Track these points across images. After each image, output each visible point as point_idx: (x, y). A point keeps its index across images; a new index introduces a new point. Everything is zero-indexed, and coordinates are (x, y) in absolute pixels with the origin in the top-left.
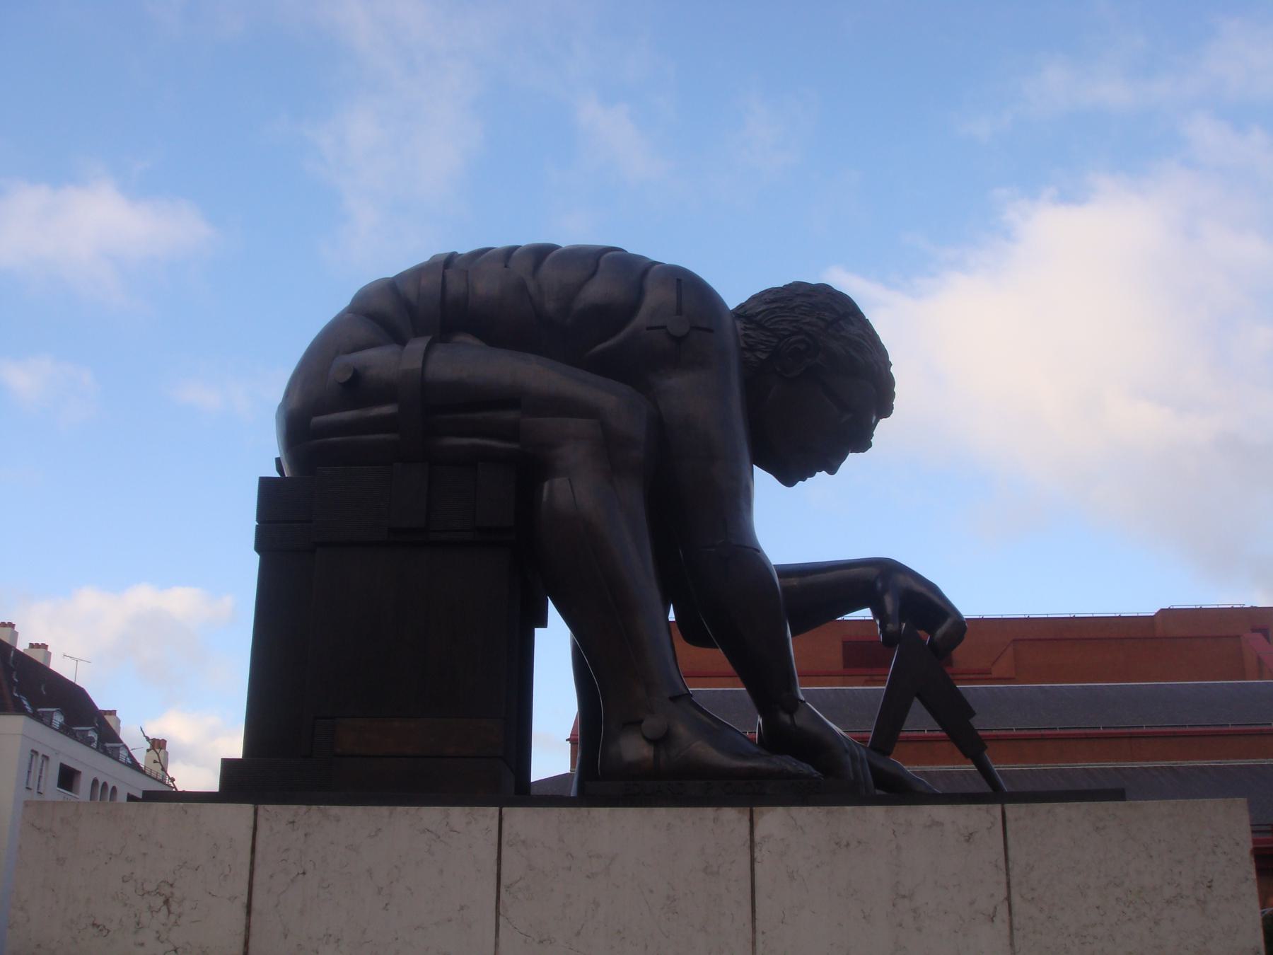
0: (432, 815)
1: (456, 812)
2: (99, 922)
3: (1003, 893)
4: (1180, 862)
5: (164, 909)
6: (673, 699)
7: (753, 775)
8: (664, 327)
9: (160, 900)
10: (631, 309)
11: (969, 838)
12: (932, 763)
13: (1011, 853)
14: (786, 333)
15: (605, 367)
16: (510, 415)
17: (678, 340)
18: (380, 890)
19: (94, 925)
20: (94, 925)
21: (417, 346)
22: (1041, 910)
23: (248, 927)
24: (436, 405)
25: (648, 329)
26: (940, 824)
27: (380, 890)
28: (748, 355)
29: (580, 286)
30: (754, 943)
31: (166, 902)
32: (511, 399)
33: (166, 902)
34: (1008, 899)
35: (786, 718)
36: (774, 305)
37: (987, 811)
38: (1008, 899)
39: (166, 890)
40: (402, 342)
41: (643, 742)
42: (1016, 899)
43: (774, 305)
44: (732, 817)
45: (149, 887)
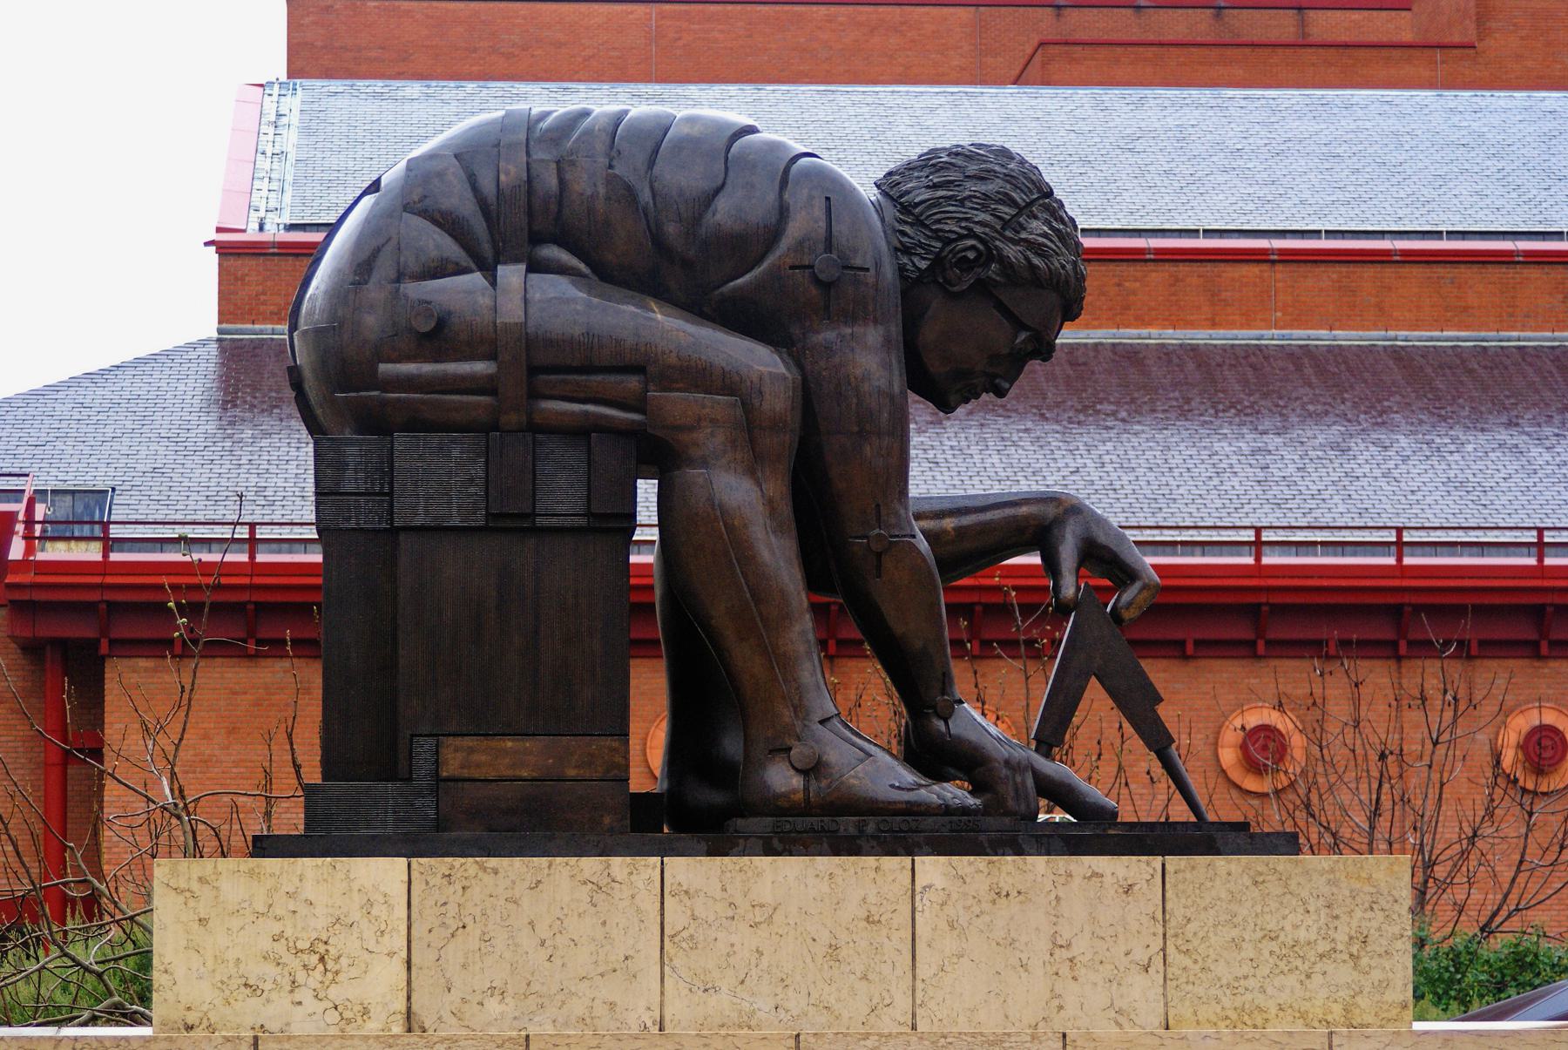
1: (616, 861)
2: (251, 982)
4: (1337, 917)
5: (321, 967)
6: (822, 722)
7: (914, 810)
8: (812, 267)
9: (315, 959)
10: (773, 234)
11: (1128, 890)
13: (1169, 906)
16: (633, 382)
17: (826, 286)
18: (543, 943)
19: (246, 985)
20: (246, 985)
21: (511, 274)
22: (1196, 962)
23: (409, 982)
24: (543, 361)
25: (792, 268)
26: (1096, 875)
27: (543, 943)
30: (914, 991)
31: (322, 959)
32: (639, 364)
33: (322, 959)
34: (1164, 949)
35: (941, 725)
36: (940, 193)
37: (1148, 864)
38: (1164, 949)
39: (321, 948)
40: (488, 269)
41: (792, 772)
42: (1171, 949)
43: (940, 193)
44: (895, 865)
45: (300, 945)
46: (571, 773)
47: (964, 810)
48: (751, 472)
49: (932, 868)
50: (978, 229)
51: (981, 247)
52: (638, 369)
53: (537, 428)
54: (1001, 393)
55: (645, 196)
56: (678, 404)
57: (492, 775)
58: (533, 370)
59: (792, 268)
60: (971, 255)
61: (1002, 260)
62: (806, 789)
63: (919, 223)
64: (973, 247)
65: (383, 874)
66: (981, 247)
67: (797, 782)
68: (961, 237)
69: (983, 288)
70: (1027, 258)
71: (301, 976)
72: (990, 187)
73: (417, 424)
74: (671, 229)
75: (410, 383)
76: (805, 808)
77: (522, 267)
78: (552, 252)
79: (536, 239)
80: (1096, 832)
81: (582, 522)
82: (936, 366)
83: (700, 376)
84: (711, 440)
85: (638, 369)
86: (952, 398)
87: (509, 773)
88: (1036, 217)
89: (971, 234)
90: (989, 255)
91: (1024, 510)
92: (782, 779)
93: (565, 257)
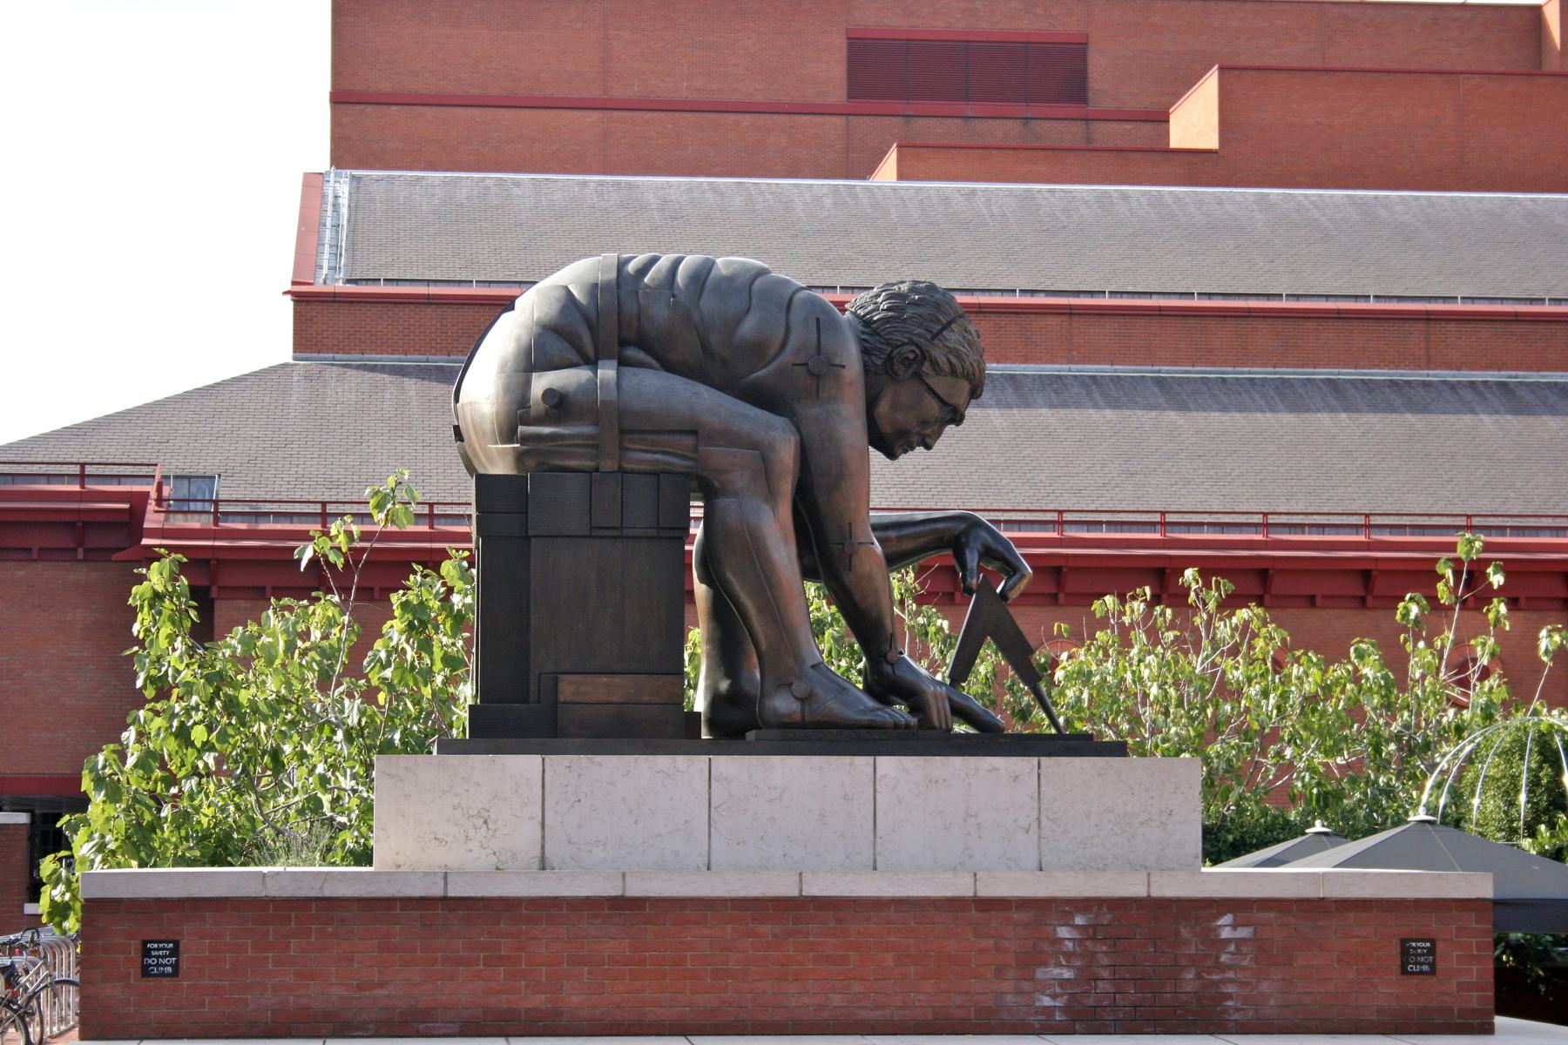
0: (663, 761)
1: (680, 758)
3: (1035, 815)
7: (871, 726)
15: (764, 398)
16: (688, 440)
23: (543, 837)
24: (626, 424)
26: (995, 769)
27: (631, 811)
29: (738, 321)
31: (485, 822)
34: (1039, 819)
38: (1039, 819)
39: (485, 814)
42: (1043, 819)
44: (863, 762)
46: (646, 699)
47: (907, 726)
49: (887, 764)
50: (915, 339)
52: (695, 433)
53: (622, 471)
54: (928, 447)
55: (696, 317)
56: (718, 455)
57: (593, 700)
58: (623, 432)
60: (911, 356)
62: (803, 711)
63: (875, 333)
65: (524, 766)
67: (796, 706)
68: (904, 344)
71: (472, 833)
72: (921, 310)
74: (714, 339)
76: (802, 725)
77: (615, 363)
78: (632, 352)
79: (623, 343)
80: (990, 739)
81: (653, 532)
82: (886, 427)
83: (729, 438)
84: (739, 479)
87: (605, 699)
89: (911, 342)
91: (941, 525)
92: (783, 704)
93: (641, 355)
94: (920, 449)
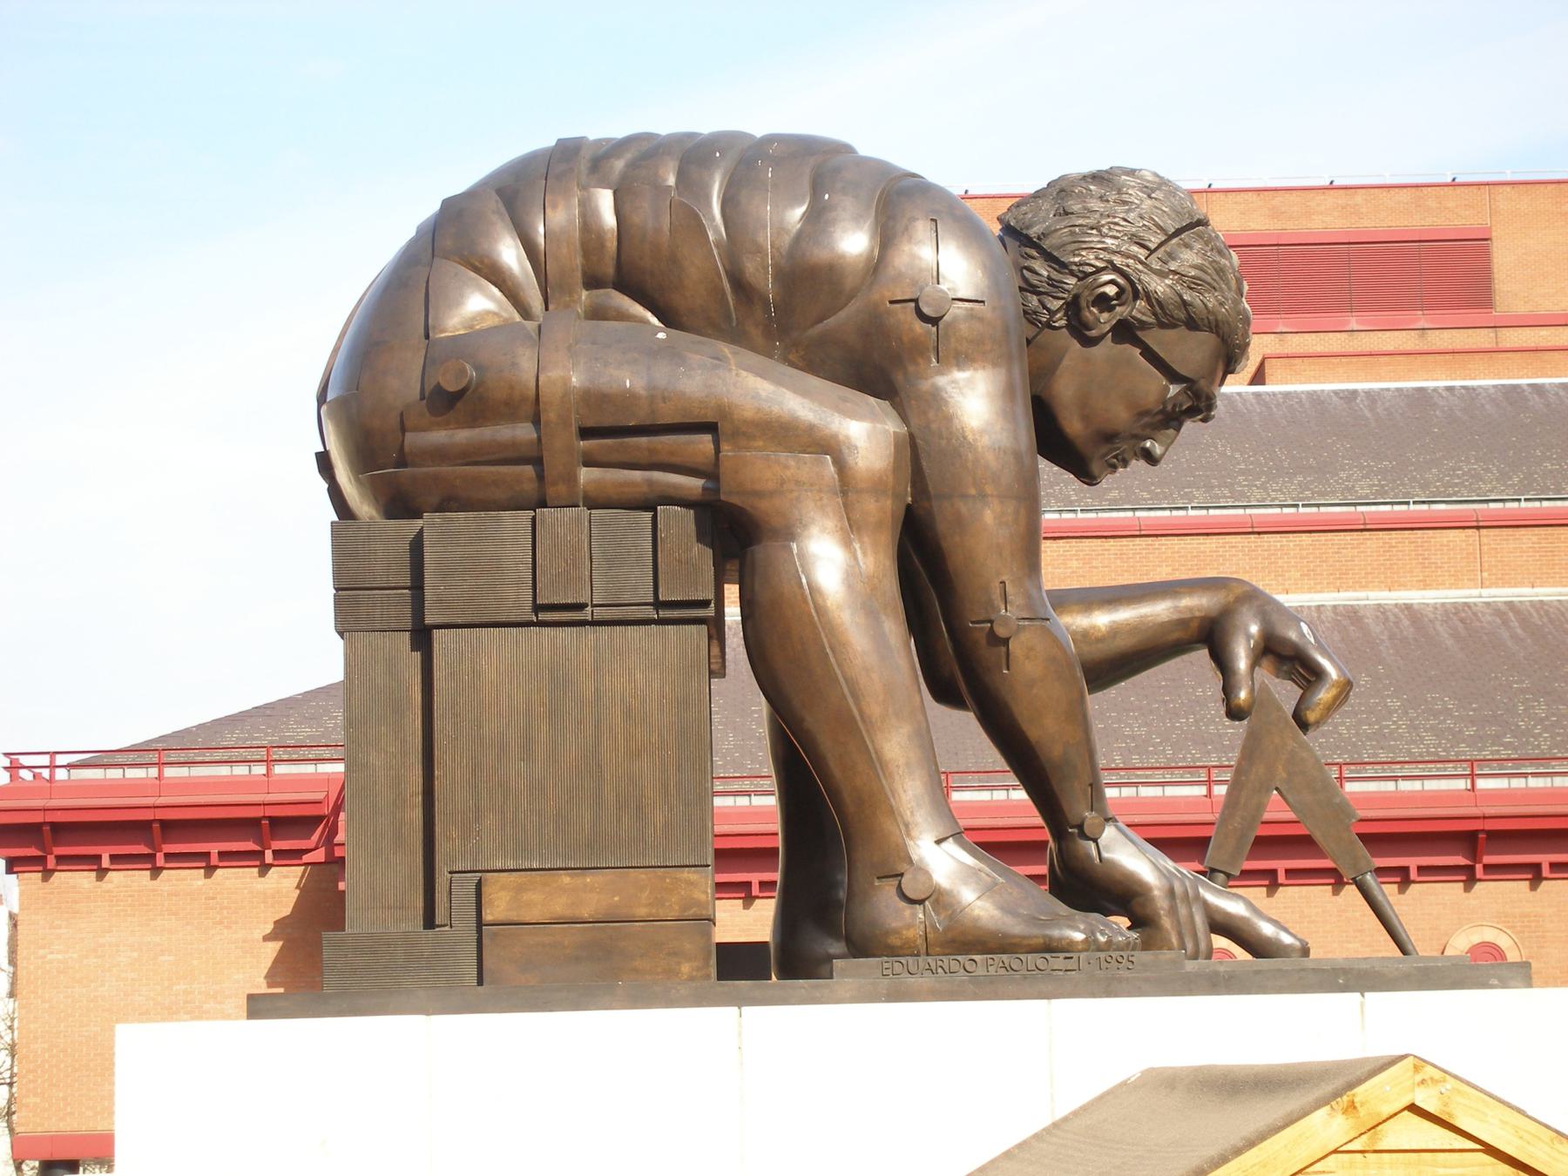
12: (1425, 585)
14: (1090, 270)
16: (705, 442)
25: (892, 302)
28: (1034, 301)
46: (642, 912)
48: (847, 544)
50: (1118, 260)
51: (1121, 281)
52: (710, 428)
59: (892, 302)
60: (1111, 290)
61: (1148, 296)
64: (1112, 282)
66: (1121, 281)
68: (1099, 270)
69: (1125, 332)
70: (1181, 296)
73: (450, 502)
75: (441, 455)
82: (1073, 425)
85: (710, 428)
86: (1095, 467)
88: (1187, 246)
90: (1132, 290)
94: (1138, 465)
